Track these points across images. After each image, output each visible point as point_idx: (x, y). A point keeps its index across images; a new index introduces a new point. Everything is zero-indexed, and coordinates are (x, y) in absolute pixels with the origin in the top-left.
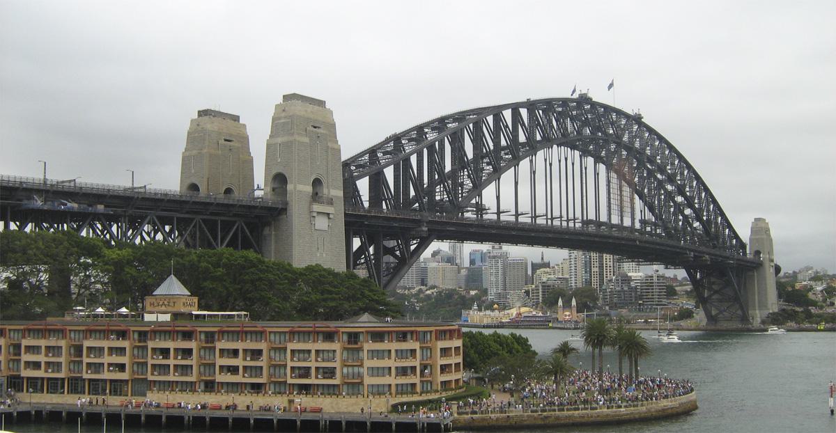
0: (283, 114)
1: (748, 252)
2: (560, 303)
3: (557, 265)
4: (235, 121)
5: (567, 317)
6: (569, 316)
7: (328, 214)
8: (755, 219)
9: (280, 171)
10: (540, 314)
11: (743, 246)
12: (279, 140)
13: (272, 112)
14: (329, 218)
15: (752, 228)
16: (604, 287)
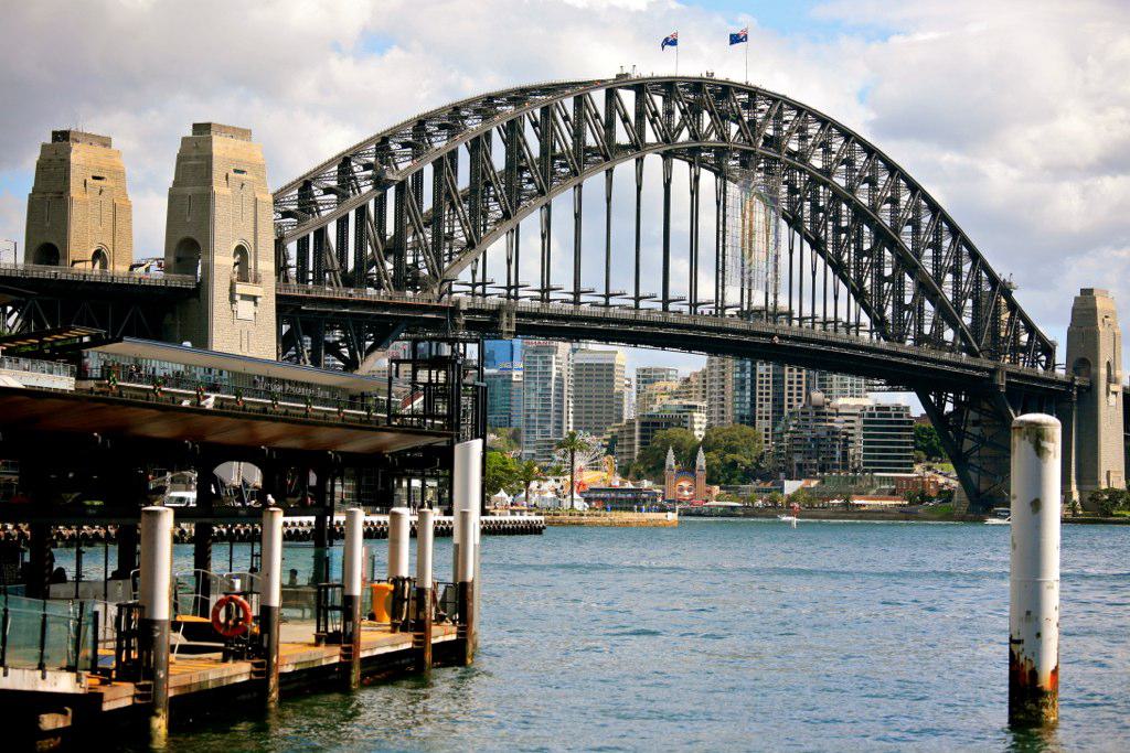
0: (194, 154)
1: (1061, 356)
2: (671, 458)
3: (696, 375)
4: (105, 145)
5: (686, 493)
6: (689, 490)
7: (254, 299)
8: (1083, 291)
9: (191, 235)
10: (629, 485)
11: (1049, 349)
12: (189, 190)
13: (176, 148)
14: (256, 304)
15: (1074, 310)
16: (778, 429)
